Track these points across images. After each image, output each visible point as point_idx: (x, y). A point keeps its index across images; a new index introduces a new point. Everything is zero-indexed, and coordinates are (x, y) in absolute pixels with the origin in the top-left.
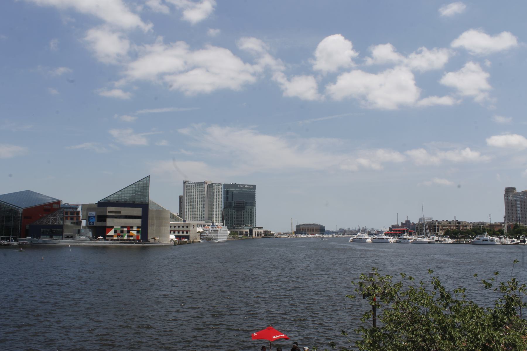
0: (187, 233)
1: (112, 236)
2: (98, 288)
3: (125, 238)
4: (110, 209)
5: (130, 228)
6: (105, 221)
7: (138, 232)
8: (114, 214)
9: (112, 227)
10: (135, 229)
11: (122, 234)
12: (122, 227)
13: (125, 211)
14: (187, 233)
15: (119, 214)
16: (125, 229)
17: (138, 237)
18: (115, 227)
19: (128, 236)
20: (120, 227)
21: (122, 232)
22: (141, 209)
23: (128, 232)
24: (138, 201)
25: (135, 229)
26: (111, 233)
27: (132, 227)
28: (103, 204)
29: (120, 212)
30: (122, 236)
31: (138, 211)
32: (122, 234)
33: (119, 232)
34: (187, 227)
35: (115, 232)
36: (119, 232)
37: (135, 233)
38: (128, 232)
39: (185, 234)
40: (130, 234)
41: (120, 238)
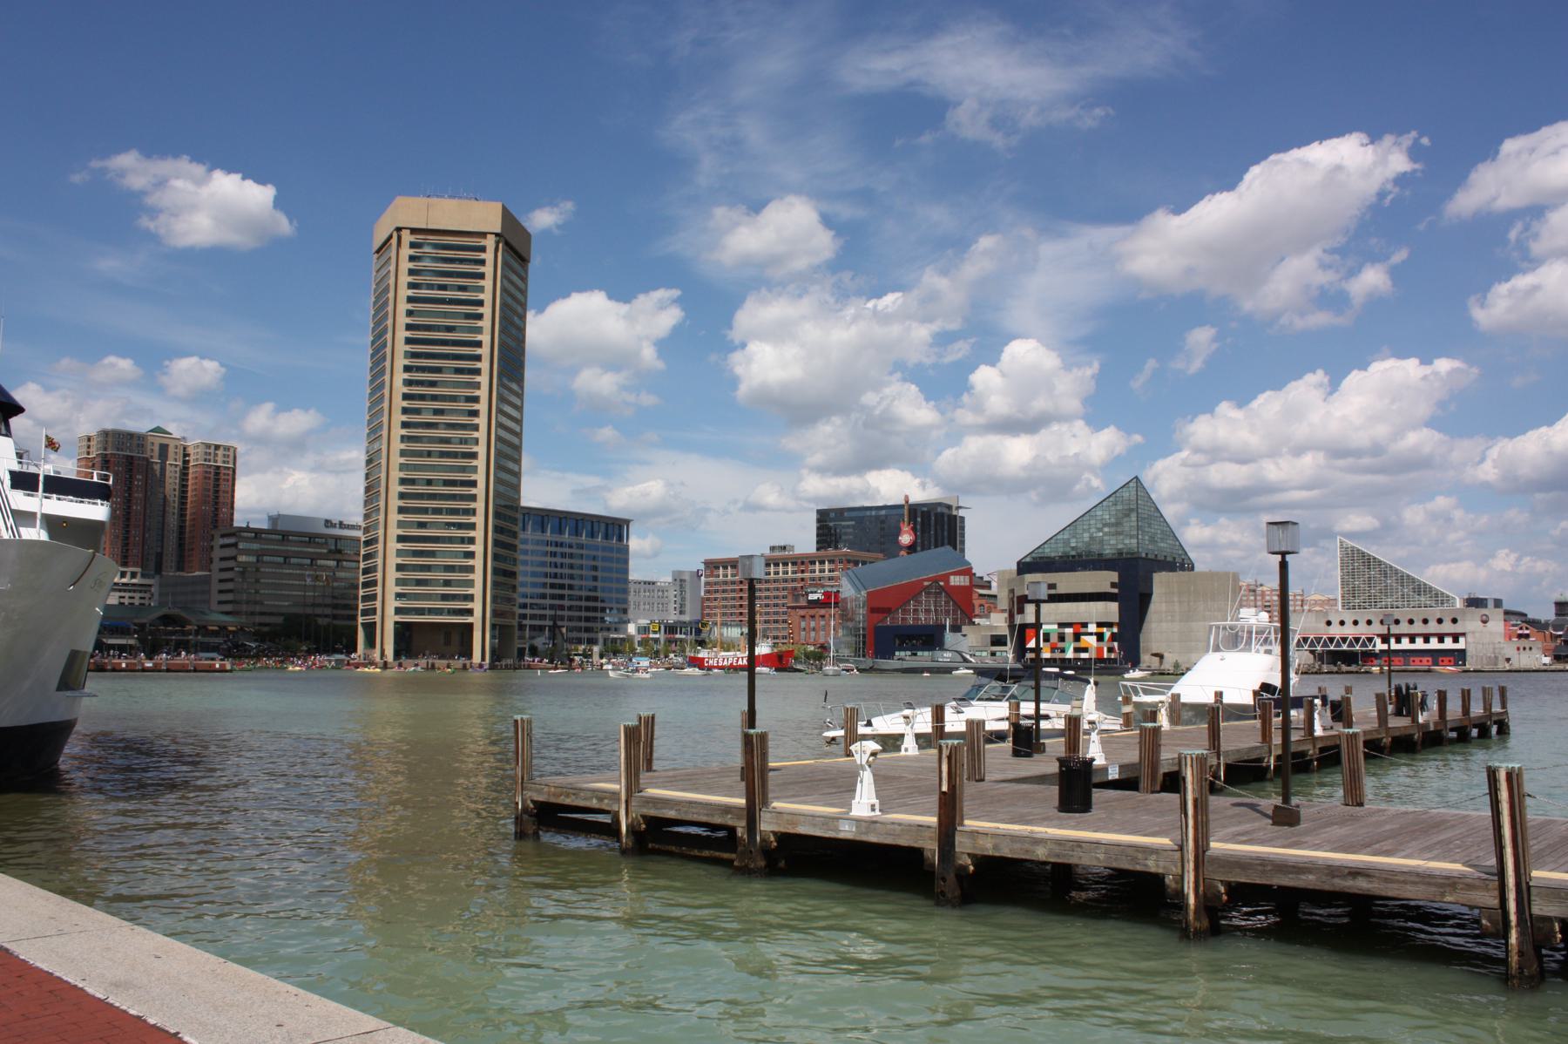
0: (1456, 640)
3: (1070, 654)
5: (1080, 628)
7: (1100, 637)
10: (1092, 628)
11: (1060, 645)
12: (1061, 625)
13: (1068, 582)
14: (1456, 640)
16: (1069, 631)
17: (1100, 650)
19: (1077, 650)
21: (1062, 638)
23: (1077, 637)
24: (1108, 551)
25: (1092, 628)
27: (1085, 625)
30: (1063, 651)
31: (1104, 580)
32: (1060, 645)
33: (1054, 638)
34: (1454, 621)
36: (1054, 638)
38: (1077, 637)
39: (1448, 644)
40: (1081, 645)
41: (1058, 655)
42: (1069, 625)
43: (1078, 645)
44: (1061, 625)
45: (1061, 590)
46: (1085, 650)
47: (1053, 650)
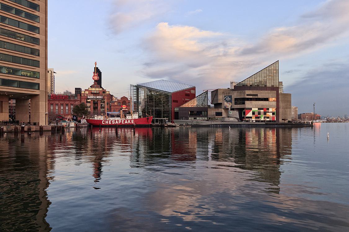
1: (251, 118)
2: (208, 161)
3: (262, 119)
4: (248, 92)
5: (266, 111)
6: (244, 103)
7: (273, 114)
8: (251, 97)
9: (251, 109)
15: (256, 97)
16: (262, 111)
17: (273, 118)
18: (253, 109)
20: (257, 109)
21: (259, 113)
22: (276, 91)
23: (265, 113)
25: (271, 110)
26: (250, 114)
27: (268, 109)
28: (240, 87)
29: (257, 95)
32: (259, 116)
33: (256, 114)
35: (253, 113)
36: (256, 114)
37: (271, 114)
38: (265, 113)
40: (267, 116)
42: (262, 109)
43: (265, 116)
44: (259, 109)
45: (260, 96)
46: (268, 118)
47: (256, 117)
